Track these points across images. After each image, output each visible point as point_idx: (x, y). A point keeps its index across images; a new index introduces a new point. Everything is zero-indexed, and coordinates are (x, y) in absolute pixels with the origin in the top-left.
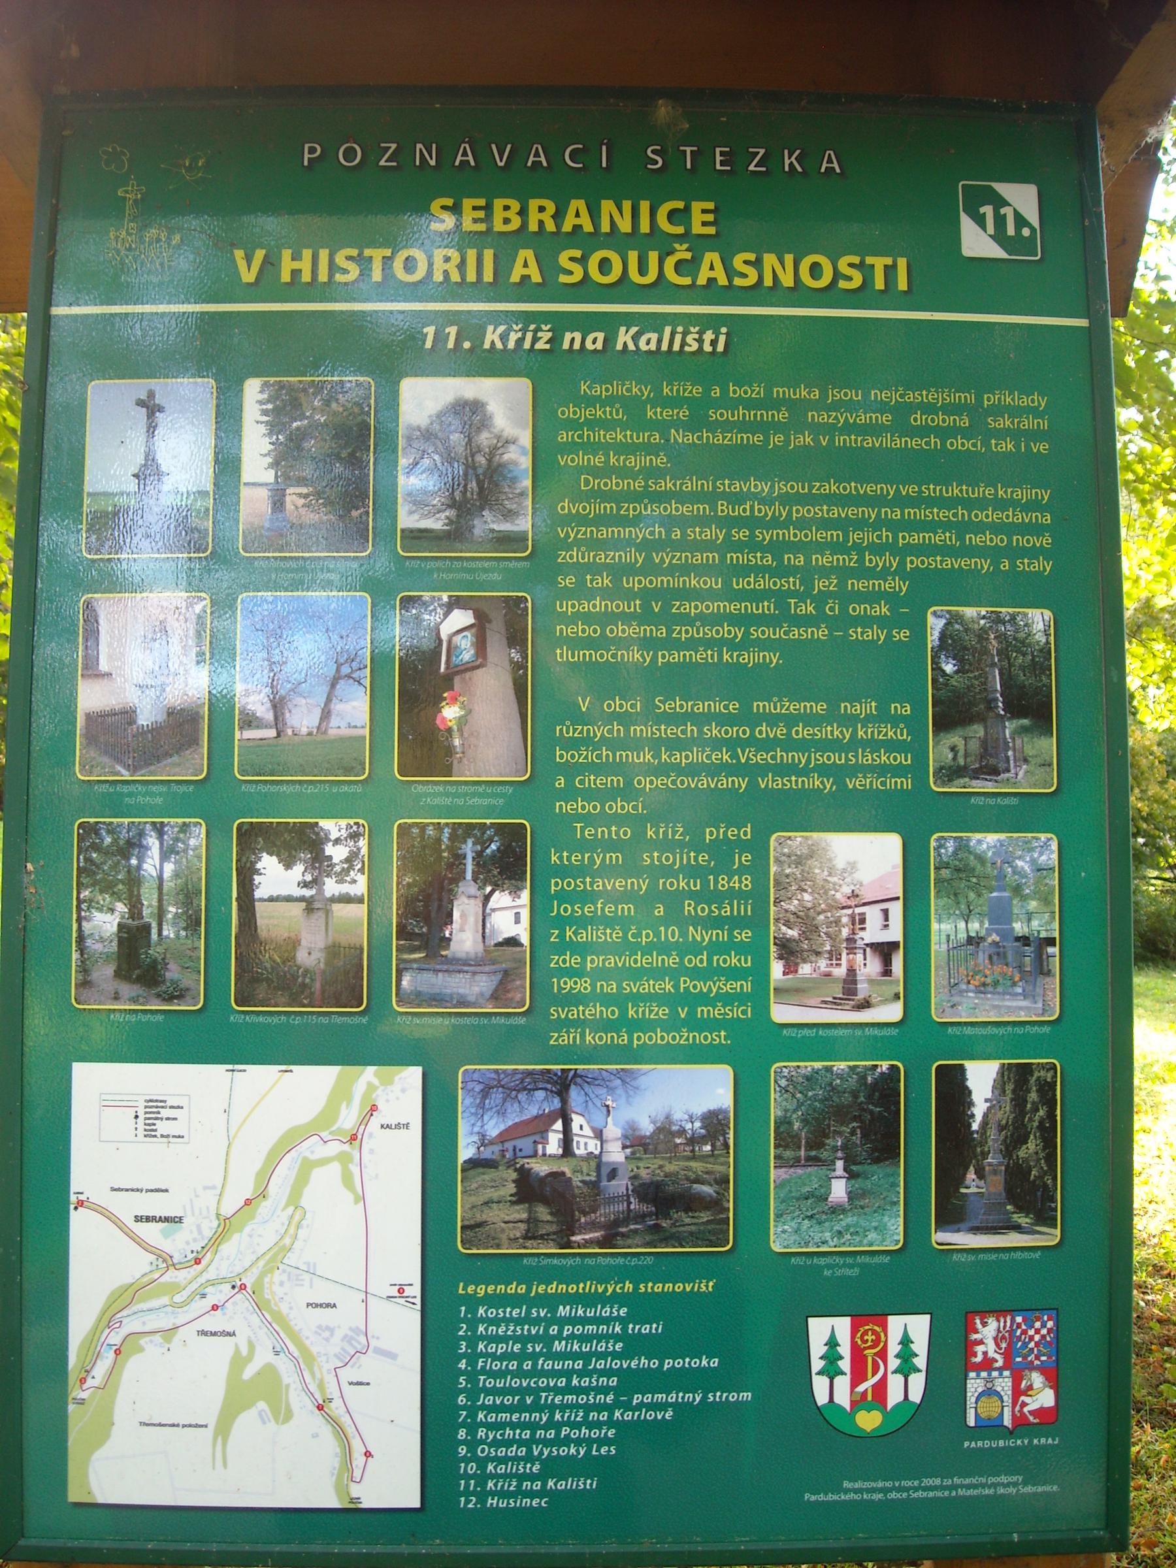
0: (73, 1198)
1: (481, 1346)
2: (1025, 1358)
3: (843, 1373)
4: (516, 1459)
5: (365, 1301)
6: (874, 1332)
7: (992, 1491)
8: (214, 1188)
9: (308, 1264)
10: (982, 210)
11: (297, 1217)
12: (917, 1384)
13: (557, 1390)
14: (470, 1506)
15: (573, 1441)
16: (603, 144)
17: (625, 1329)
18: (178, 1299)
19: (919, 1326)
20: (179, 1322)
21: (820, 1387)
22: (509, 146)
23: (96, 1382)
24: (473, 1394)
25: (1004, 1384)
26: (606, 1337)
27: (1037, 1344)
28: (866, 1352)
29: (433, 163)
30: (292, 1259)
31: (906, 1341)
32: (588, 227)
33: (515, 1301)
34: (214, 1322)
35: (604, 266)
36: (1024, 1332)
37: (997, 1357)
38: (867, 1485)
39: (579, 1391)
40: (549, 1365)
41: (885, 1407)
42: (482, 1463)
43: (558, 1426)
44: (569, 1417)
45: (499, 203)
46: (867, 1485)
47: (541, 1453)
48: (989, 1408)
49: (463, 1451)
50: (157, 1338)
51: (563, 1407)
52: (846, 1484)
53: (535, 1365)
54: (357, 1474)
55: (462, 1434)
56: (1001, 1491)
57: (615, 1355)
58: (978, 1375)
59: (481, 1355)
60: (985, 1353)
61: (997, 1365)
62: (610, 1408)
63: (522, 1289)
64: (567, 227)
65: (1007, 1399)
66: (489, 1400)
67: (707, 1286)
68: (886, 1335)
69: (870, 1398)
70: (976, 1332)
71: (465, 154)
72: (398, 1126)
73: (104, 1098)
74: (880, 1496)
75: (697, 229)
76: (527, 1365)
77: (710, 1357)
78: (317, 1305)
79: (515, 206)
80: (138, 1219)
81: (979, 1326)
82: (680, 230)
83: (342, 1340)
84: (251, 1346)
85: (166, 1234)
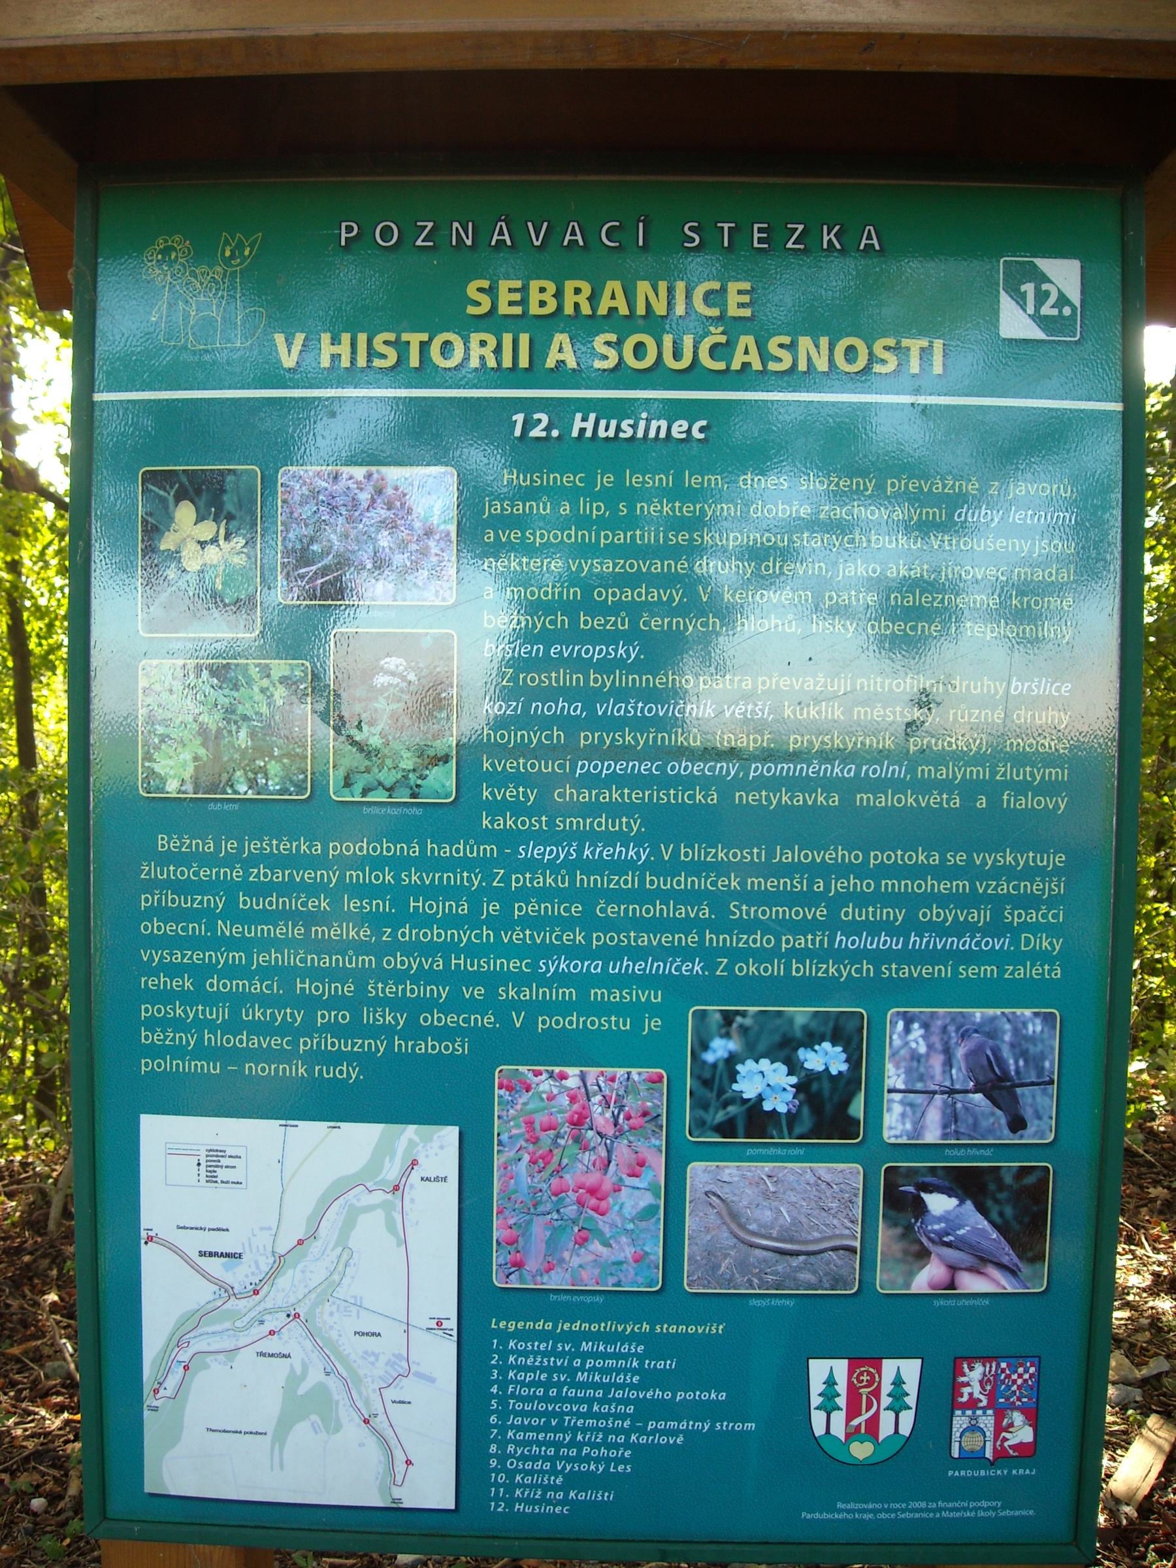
0: (144, 1234)
1: (511, 1374)
2: (1007, 1399)
3: (839, 1409)
4: (542, 1472)
5: (407, 1331)
6: (869, 1373)
7: (973, 1514)
8: (270, 1228)
9: (355, 1298)
10: (1023, 288)
11: (345, 1257)
12: (907, 1420)
13: (579, 1415)
14: (500, 1510)
15: (593, 1459)
16: (639, 221)
17: (641, 1364)
18: (238, 1324)
19: (911, 1370)
20: (240, 1344)
21: (818, 1420)
22: (545, 224)
23: (168, 1393)
24: (504, 1414)
25: (987, 1421)
26: (625, 1371)
27: (1019, 1387)
28: (862, 1391)
29: (469, 242)
30: (341, 1293)
31: (898, 1382)
32: (624, 310)
33: (543, 1336)
34: (272, 1345)
35: (639, 349)
36: (1008, 1376)
37: (982, 1397)
38: (858, 1506)
39: (599, 1416)
40: (572, 1393)
41: (877, 1439)
42: (511, 1474)
43: (580, 1446)
44: (590, 1438)
45: (534, 285)
46: (858, 1506)
47: (564, 1468)
48: (972, 1442)
49: (493, 1463)
50: (221, 1357)
51: (584, 1430)
52: (840, 1505)
53: (559, 1392)
54: (399, 1479)
55: (493, 1448)
56: (981, 1514)
57: (632, 1386)
58: (963, 1413)
59: (512, 1381)
60: (971, 1394)
61: (981, 1405)
62: (627, 1433)
63: (549, 1326)
64: (602, 310)
65: (990, 1435)
66: (518, 1421)
67: (717, 1329)
68: (880, 1376)
69: (863, 1430)
70: (964, 1375)
71: (501, 233)
72: (437, 1179)
73: (169, 1146)
74: (871, 1516)
75: (733, 311)
76: (553, 1392)
77: (718, 1391)
78: (363, 1334)
79: (551, 288)
80: (202, 1254)
81: (966, 1370)
82: (715, 312)
83: (386, 1364)
84: (305, 1367)
85: (227, 1268)
